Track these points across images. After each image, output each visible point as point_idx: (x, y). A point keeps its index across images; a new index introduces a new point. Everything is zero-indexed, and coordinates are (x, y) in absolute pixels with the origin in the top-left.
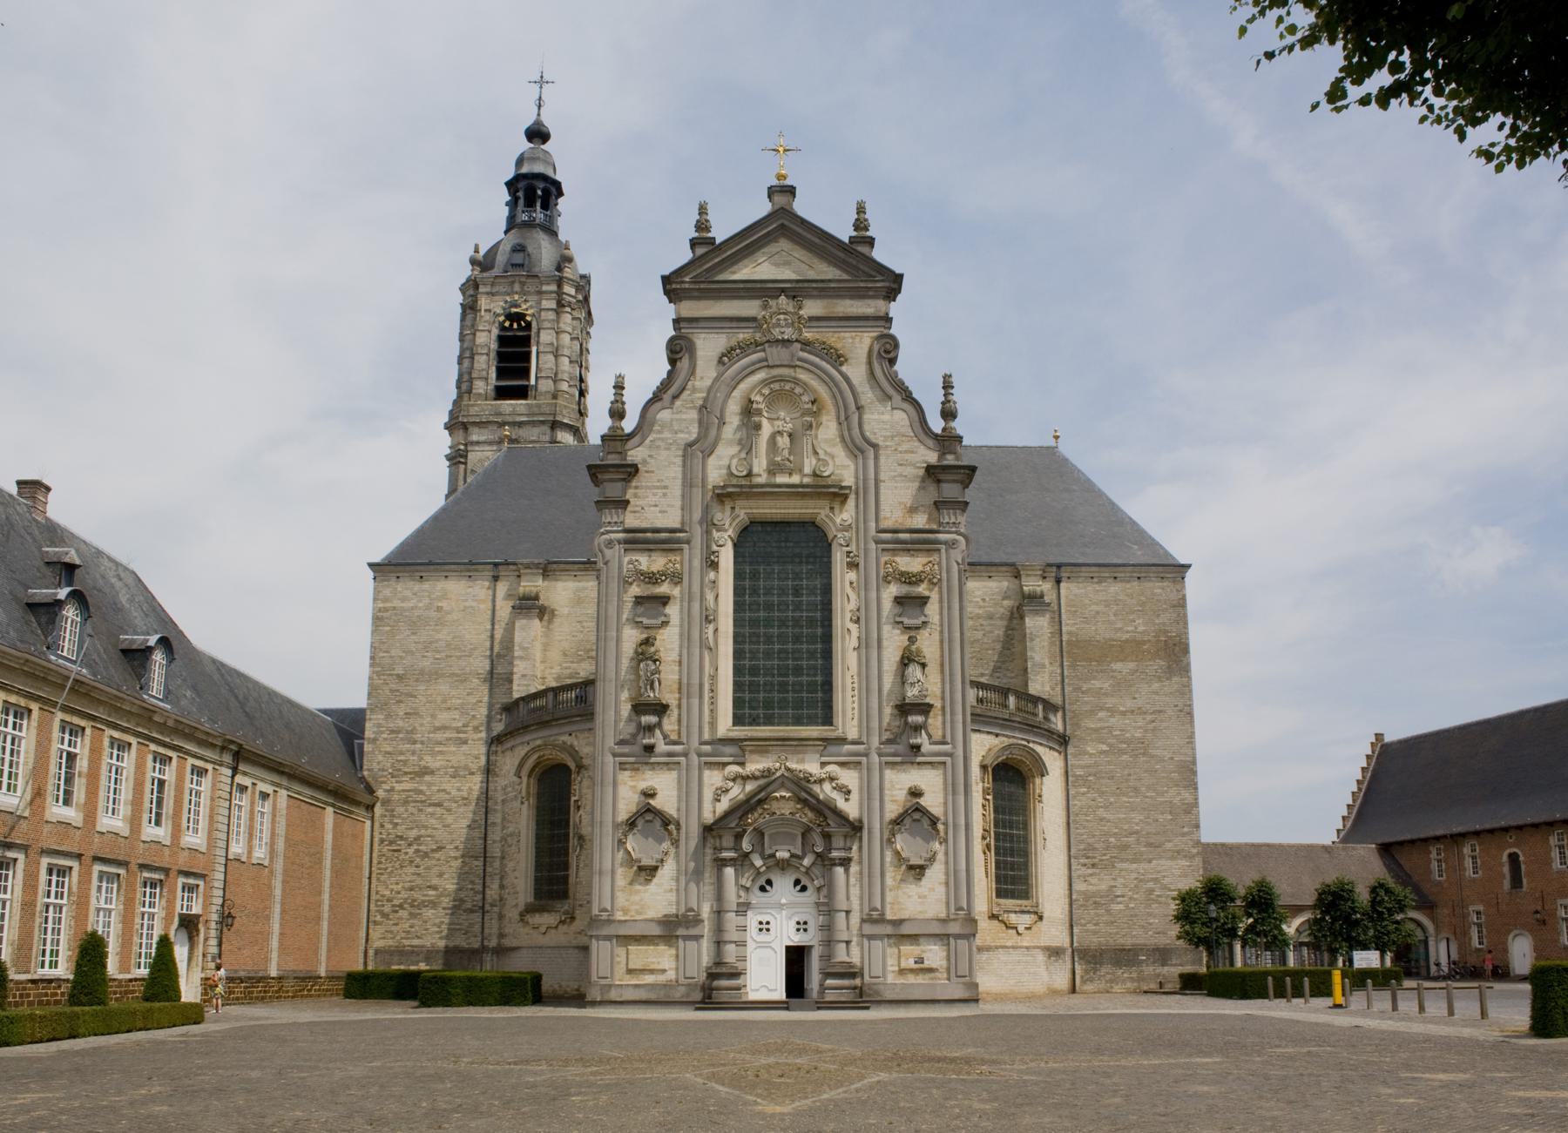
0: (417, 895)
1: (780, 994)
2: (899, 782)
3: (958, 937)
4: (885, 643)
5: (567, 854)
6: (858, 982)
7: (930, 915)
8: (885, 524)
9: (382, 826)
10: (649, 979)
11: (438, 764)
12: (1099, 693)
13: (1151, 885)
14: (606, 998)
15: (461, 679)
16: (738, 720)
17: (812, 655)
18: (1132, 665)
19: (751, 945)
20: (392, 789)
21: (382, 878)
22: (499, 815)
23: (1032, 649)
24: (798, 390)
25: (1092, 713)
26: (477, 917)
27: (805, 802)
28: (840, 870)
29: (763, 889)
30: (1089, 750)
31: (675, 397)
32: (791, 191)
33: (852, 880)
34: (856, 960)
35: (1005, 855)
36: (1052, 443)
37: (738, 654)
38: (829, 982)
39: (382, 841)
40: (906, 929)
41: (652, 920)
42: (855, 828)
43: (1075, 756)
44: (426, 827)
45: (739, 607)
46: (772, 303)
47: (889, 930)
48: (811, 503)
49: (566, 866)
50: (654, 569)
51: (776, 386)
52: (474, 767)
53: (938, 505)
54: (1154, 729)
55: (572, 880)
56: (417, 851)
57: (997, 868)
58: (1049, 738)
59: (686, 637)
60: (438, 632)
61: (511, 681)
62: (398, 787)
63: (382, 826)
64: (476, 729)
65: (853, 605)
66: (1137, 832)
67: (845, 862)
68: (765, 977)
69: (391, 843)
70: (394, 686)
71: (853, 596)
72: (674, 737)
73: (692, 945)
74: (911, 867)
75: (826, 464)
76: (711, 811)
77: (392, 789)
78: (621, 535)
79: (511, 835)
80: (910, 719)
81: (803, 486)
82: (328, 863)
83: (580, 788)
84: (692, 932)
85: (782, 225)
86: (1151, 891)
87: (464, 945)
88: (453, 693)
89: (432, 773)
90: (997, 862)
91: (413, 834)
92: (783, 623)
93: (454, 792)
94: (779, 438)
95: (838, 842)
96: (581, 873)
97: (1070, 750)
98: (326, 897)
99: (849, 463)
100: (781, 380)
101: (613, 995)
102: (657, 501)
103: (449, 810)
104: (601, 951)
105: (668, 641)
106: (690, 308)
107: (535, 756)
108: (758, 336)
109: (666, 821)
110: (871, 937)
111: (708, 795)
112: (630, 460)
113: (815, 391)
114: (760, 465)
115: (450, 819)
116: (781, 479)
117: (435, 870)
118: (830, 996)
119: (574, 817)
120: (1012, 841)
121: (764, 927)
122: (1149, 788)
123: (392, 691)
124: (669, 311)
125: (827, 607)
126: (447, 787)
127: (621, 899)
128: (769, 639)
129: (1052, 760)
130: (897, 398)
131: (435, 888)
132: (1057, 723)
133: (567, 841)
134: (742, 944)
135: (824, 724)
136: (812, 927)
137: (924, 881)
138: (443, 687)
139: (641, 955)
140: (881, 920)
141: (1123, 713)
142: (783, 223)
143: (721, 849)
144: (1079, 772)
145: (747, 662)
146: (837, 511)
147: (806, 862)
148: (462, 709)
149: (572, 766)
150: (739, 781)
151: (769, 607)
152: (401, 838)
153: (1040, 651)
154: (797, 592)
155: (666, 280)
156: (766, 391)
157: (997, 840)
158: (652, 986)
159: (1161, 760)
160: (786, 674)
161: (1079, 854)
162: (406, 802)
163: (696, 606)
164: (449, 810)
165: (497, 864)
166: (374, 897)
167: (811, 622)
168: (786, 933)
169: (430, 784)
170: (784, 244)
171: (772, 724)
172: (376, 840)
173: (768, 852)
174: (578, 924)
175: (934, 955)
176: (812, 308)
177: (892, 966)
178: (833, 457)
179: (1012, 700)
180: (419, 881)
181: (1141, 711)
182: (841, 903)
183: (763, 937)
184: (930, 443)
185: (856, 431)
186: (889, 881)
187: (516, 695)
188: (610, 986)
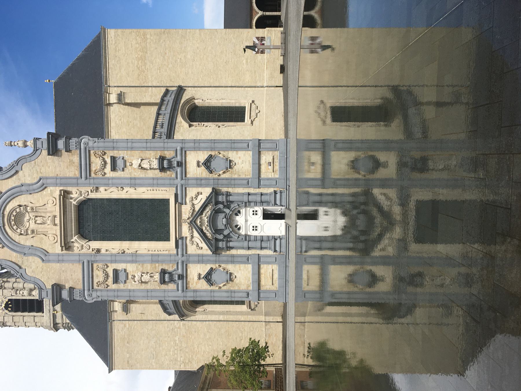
2: (193, 170)
4: (133, 176)
8: (78, 174)
10: (276, 276)
19: (262, 234)
24: (14, 213)
27: (202, 213)
29: (239, 229)
31: (20, 267)
38: (278, 202)
51: (13, 223)
53: (68, 150)
59: (132, 262)
71: (112, 189)
72: (175, 267)
73: (262, 259)
76: (206, 250)
80: (165, 166)
94: (38, 222)
99: (49, 190)
111: (200, 252)
112: (50, 287)
116: (57, 221)
121: (255, 228)
127: (243, 287)
130: (16, 168)
137: (236, 161)
146: (72, 196)
150: (193, 240)
156: (15, 227)
173: (223, 227)
175: (266, 157)
177: (271, 175)
183: (259, 228)
185: (35, 186)
186: (236, 176)
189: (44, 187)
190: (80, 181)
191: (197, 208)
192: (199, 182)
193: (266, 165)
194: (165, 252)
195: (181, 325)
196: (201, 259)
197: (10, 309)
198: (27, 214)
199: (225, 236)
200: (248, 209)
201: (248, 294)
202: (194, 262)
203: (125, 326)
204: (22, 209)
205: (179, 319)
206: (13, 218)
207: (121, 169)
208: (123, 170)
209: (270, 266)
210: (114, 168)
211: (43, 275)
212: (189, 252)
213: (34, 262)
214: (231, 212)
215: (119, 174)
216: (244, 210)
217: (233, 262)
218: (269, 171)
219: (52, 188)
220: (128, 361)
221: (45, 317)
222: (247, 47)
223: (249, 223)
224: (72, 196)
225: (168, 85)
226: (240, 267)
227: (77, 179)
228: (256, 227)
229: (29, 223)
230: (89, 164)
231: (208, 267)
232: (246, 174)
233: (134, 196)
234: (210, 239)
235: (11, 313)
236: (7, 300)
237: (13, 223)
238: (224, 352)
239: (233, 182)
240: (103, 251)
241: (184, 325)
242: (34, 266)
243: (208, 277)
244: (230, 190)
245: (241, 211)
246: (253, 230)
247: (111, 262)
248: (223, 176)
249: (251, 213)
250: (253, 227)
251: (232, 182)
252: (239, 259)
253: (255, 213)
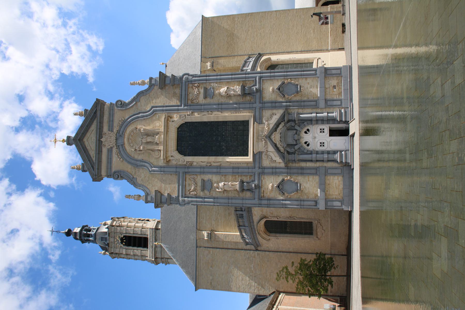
4: (220, 102)
10: (341, 186)
16: (247, 155)
29: (308, 145)
32: (69, 138)
46: (103, 143)
59: (217, 173)
61: (237, 242)
73: (330, 171)
85: (79, 140)
100: (128, 139)
106: (103, 173)
111: (274, 165)
121: (322, 144)
124: (105, 179)
147: (297, 127)
155: (94, 180)
163: (206, 170)
170: (85, 140)
176: (105, 129)
183: (326, 144)
184: (153, 87)
186: (305, 99)
190: (179, 108)
191: (271, 126)
192: (274, 105)
193: (331, 88)
194: (243, 165)
195: (256, 254)
196: (274, 171)
197: (124, 243)
201: (316, 202)
202: (269, 174)
203: (209, 252)
205: (254, 249)
208: (213, 98)
210: (205, 97)
211: (149, 183)
213: (143, 172)
215: (208, 100)
217: (302, 174)
218: (334, 93)
219: (159, 114)
220: (211, 283)
221: (149, 252)
222: (314, 14)
223: (316, 140)
225: (250, 54)
226: (309, 179)
227: (178, 106)
228: (323, 143)
230: (187, 95)
231: (280, 179)
233: (221, 119)
234: (282, 153)
235: (125, 247)
236: (122, 236)
238: (293, 263)
239: (303, 103)
240: (195, 164)
241: (258, 254)
242: (143, 176)
243: (280, 187)
244: (300, 111)
247: (201, 173)
248: (295, 99)
249: (319, 131)
251: (302, 104)
252: (308, 171)
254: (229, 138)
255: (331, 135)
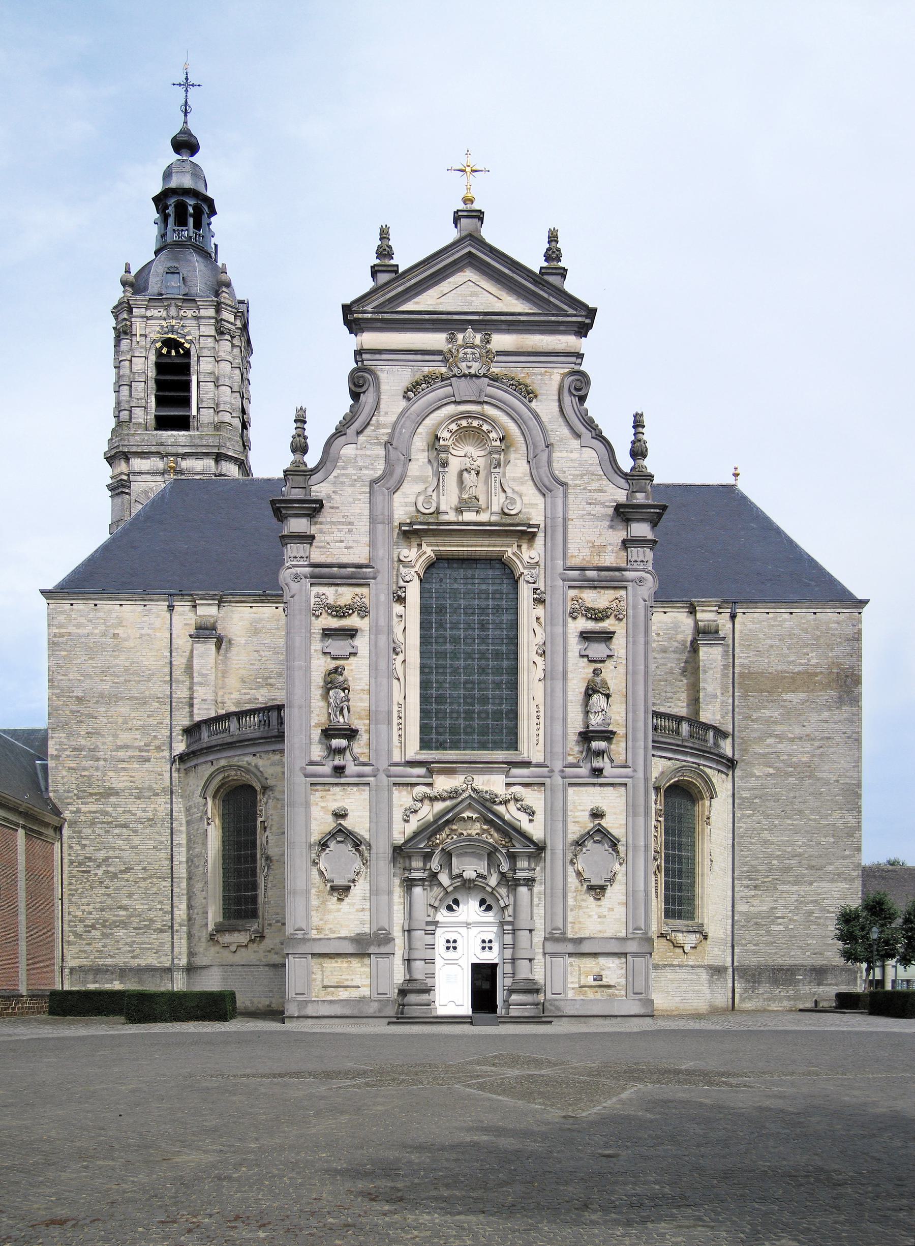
0: (106, 915)
1: (466, 1009)
3: (636, 954)
5: (254, 874)
6: (541, 998)
7: (608, 934)
9: (70, 847)
11: (122, 786)
12: (769, 721)
13: (810, 907)
14: (303, 1014)
15: (141, 702)
17: (498, 685)
18: (802, 695)
19: (439, 962)
20: (78, 811)
21: (74, 899)
22: (184, 836)
23: (705, 681)
24: (485, 427)
25: (761, 739)
26: (167, 936)
28: (523, 890)
29: (450, 908)
30: (755, 774)
33: (536, 900)
34: (538, 975)
35: (674, 876)
36: (730, 481)
37: (425, 685)
38: (515, 997)
39: (71, 862)
40: (586, 948)
41: (345, 938)
42: (538, 850)
43: (742, 778)
44: (114, 848)
45: (425, 640)
46: (460, 336)
47: (570, 948)
48: (499, 540)
49: (254, 886)
50: (342, 602)
51: (464, 423)
52: (157, 788)
54: (821, 755)
55: (261, 899)
56: (106, 872)
57: (666, 888)
58: (718, 762)
60: (116, 657)
62: (84, 808)
63: (70, 847)
64: (158, 748)
65: (540, 639)
66: (799, 855)
67: (529, 882)
68: (453, 995)
69: (80, 864)
70: (75, 708)
74: (591, 888)
75: (513, 501)
77: (78, 811)
78: (307, 569)
79: (197, 856)
81: (490, 524)
82: (22, 884)
83: (266, 809)
84: (383, 950)
86: (811, 913)
87: (155, 963)
88: (133, 714)
89: (117, 794)
90: (666, 883)
91: (102, 855)
92: (469, 656)
93: (140, 814)
94: (465, 474)
95: (522, 864)
96: (270, 893)
97: (738, 772)
98: (22, 918)
100: (467, 416)
101: (310, 1010)
102: (344, 535)
103: (135, 831)
104: (296, 968)
105: (357, 671)
107: (220, 777)
108: (444, 370)
109: (358, 844)
110: (554, 955)
113: (504, 428)
114: (448, 501)
115: (136, 840)
116: (469, 516)
117: (125, 891)
118: (514, 1012)
119: (261, 839)
120: (680, 863)
121: (451, 945)
122: (813, 811)
123: (72, 712)
125: (514, 641)
126: (133, 808)
127: (315, 920)
128: (455, 671)
129: (722, 784)
131: (125, 908)
132: (726, 748)
133: (254, 860)
134: (431, 961)
135: (508, 749)
136: (496, 946)
138: (124, 709)
139: (335, 971)
140: (563, 939)
141: (792, 740)
142: (471, 251)
143: (410, 870)
144: (746, 794)
145: (433, 691)
146: (524, 547)
148: (143, 729)
149: (258, 788)
151: (455, 640)
152: (90, 859)
153: (712, 683)
154: (483, 626)
156: (454, 427)
157: (667, 861)
158: (346, 1001)
159: (826, 783)
160: (470, 700)
161: (745, 875)
162: (93, 824)
164: (135, 831)
165: (184, 885)
166: (66, 918)
167: (497, 655)
168: (472, 952)
169: (115, 806)
171: (458, 748)
172: (66, 861)
174: (268, 943)
176: (501, 341)
177: (573, 982)
178: (521, 496)
179: (685, 727)
180: (110, 902)
181: (810, 738)
182: (523, 922)
183: (451, 954)
186: (571, 902)
187: (197, 718)
188: (307, 1002)
189: (543, 490)
193: (596, 970)
198: (483, 453)
199: (434, 875)
200: (495, 929)
204: (494, 444)
206: (475, 423)
207: (583, 653)
209: (368, 982)
212: (396, 792)
214: (490, 890)
216: (491, 919)
217: (374, 891)
218: (582, 977)
223: (463, 930)
224: (524, 547)
228: (455, 948)
229: (464, 454)
232: (577, 926)
237: (464, 423)
245: (491, 913)
246: (448, 941)
250: (455, 941)
253: (487, 945)
254: (470, 700)
255: (477, 969)
